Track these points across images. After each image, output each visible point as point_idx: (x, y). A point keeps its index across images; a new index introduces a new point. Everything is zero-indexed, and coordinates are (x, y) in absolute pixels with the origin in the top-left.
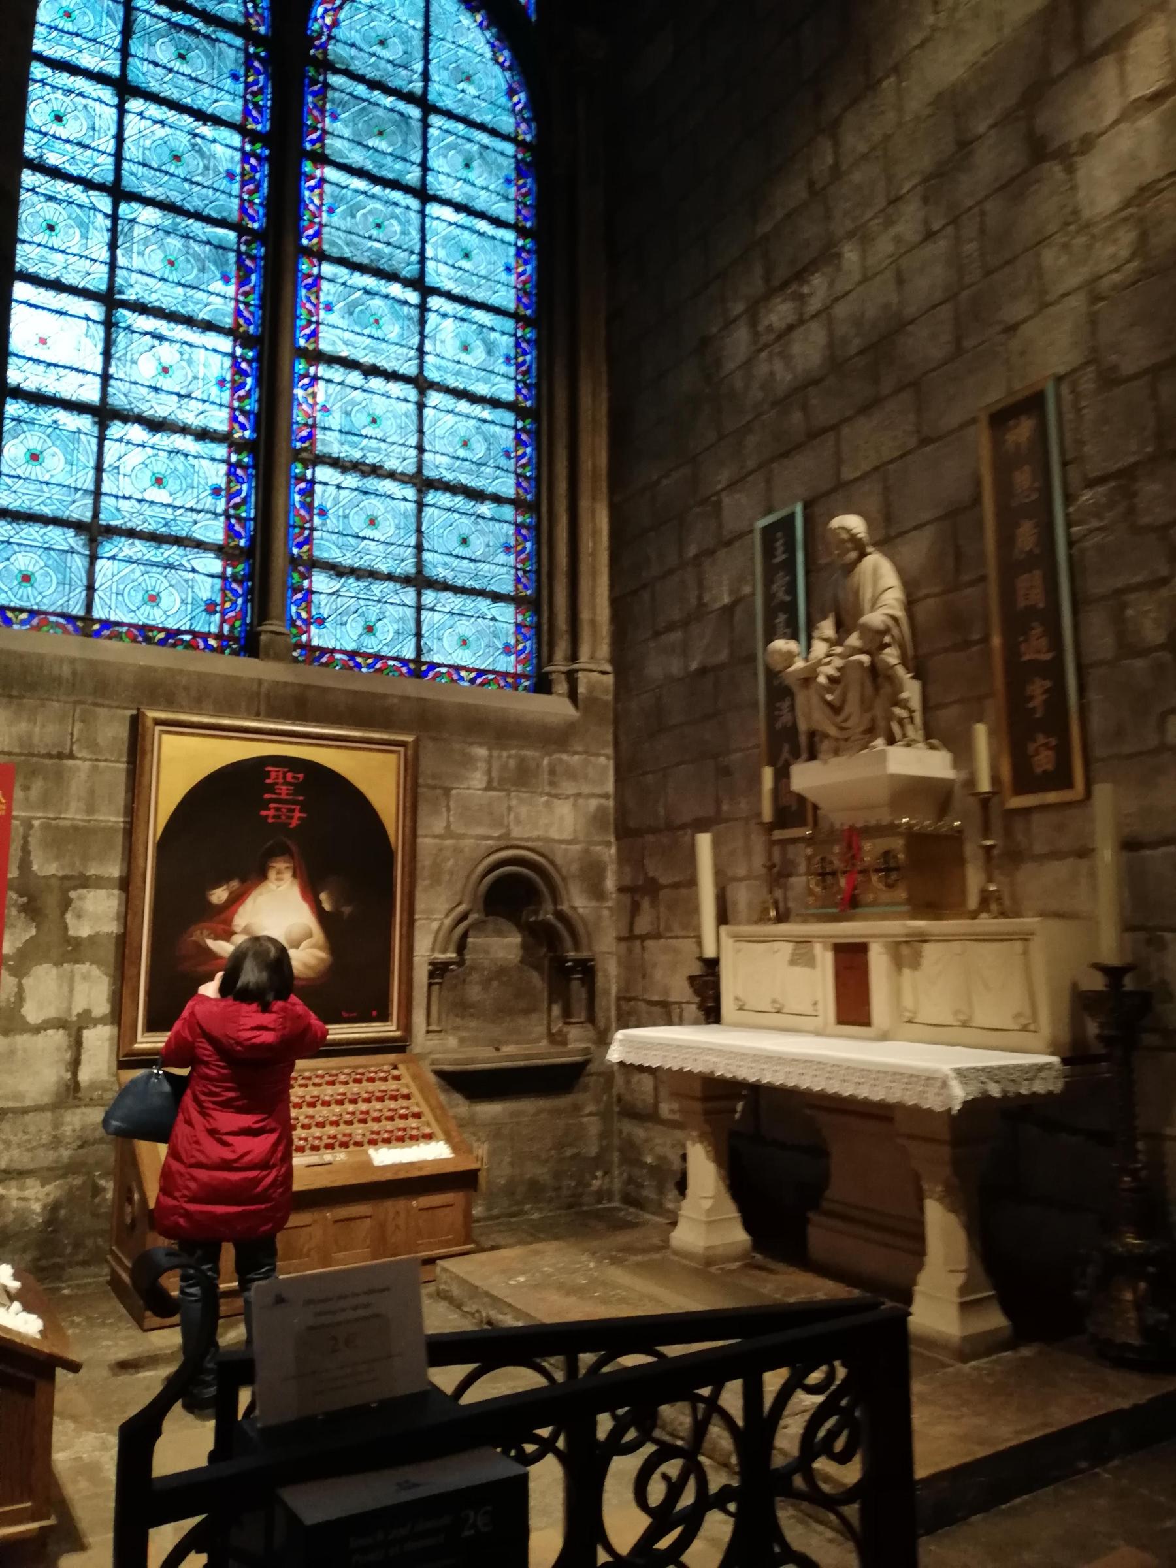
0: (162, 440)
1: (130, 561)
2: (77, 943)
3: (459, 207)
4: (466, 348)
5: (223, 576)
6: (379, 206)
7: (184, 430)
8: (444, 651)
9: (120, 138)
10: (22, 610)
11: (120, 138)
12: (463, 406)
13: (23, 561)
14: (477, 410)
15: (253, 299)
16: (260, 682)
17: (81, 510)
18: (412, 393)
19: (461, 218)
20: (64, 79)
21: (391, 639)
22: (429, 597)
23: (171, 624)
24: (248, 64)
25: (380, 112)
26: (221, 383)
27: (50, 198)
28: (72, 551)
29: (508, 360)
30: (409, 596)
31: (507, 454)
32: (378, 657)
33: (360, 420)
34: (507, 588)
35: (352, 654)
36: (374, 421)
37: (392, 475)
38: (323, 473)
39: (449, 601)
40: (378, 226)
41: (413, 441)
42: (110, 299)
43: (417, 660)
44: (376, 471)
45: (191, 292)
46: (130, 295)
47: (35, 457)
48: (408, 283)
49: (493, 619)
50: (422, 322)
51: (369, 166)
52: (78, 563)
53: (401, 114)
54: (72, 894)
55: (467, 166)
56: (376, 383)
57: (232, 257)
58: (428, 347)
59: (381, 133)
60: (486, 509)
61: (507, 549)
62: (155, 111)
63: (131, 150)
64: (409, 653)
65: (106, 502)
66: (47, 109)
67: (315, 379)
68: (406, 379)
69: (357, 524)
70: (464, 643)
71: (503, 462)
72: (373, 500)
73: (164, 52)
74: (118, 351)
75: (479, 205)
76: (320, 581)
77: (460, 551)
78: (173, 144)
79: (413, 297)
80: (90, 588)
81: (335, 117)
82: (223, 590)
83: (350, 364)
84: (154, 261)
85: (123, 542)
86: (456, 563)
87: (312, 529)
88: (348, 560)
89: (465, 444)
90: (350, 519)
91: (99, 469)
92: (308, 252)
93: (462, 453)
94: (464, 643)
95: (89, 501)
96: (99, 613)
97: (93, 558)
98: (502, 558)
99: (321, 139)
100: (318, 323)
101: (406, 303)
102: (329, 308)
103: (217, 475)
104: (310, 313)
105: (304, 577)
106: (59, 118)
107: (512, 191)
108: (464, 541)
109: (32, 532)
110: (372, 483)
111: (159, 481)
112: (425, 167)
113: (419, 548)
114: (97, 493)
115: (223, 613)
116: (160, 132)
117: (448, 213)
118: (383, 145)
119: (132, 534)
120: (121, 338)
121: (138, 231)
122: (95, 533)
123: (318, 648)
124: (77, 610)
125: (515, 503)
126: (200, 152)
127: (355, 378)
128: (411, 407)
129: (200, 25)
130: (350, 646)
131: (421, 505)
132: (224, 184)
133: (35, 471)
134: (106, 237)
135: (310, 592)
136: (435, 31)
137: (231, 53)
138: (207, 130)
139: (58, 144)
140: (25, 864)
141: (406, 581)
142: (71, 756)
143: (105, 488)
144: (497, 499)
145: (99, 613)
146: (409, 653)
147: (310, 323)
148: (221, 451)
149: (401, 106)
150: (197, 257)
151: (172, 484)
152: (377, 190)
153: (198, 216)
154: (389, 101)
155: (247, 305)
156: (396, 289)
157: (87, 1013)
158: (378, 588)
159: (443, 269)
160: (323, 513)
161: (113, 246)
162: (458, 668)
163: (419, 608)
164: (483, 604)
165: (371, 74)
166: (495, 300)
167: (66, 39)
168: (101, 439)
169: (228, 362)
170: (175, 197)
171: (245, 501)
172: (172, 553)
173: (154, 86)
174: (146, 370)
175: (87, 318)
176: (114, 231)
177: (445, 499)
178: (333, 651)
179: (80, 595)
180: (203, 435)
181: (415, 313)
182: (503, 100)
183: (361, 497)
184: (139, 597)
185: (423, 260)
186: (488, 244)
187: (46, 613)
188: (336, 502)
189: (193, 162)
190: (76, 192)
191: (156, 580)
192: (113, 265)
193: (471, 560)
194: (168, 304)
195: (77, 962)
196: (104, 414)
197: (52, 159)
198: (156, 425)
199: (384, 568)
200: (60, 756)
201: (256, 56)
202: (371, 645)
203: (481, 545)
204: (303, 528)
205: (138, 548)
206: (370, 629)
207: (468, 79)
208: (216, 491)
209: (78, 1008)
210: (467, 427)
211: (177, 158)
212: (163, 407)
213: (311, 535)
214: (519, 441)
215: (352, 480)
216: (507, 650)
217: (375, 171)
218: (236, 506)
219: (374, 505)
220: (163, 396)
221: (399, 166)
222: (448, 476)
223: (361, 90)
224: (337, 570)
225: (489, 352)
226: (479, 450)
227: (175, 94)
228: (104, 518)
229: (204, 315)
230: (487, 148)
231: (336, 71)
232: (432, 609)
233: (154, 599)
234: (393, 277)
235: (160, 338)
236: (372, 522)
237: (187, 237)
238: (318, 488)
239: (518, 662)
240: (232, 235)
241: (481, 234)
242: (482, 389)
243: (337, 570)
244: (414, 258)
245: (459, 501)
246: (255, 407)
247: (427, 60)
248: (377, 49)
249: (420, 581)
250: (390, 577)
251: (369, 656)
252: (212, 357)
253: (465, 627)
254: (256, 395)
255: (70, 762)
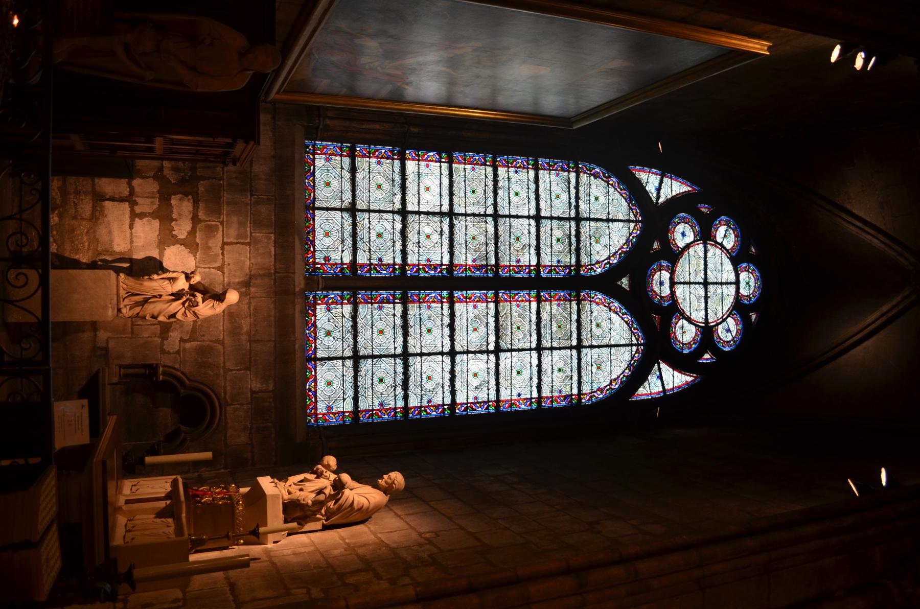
0: (398, 236)
1: (342, 225)
2: (169, 199)
3: (539, 366)
4: (475, 375)
5: (342, 264)
6: (527, 328)
7: (404, 245)
8: (324, 373)
9: (517, 217)
10: (314, 183)
11: (517, 217)
12: (447, 376)
13: (335, 183)
14: (447, 383)
15: (469, 273)
16: (294, 273)
17: (360, 205)
18: (447, 349)
19: (535, 370)
20: (532, 197)
21: (325, 345)
22: (349, 363)
23: (317, 242)
24: (565, 267)
25: (568, 326)
26: (429, 260)
27: (485, 191)
28: (342, 201)
29: (476, 398)
30: (348, 353)
31: (429, 401)
32: (315, 338)
33: (428, 324)
34: (362, 406)
35: (315, 325)
36: (429, 331)
37: (405, 342)
38: (399, 308)
39: (350, 373)
40: (518, 328)
41: (424, 351)
42: (451, 214)
43: (316, 359)
44: (406, 334)
45: (464, 246)
46: (456, 222)
47: (379, 187)
48: (497, 343)
49: (344, 399)
50: (481, 352)
51: (543, 322)
52: (338, 204)
53: (571, 336)
54: (190, 197)
55: (560, 370)
56: (447, 331)
57: (484, 263)
58: (470, 356)
59: (559, 327)
60: (399, 390)
61: (381, 404)
62: (533, 230)
63: (514, 221)
64: (319, 354)
65: (366, 215)
66: (519, 190)
67: (442, 303)
68: (453, 345)
69: (379, 325)
70: (329, 383)
71: (425, 399)
72: (392, 332)
73: (558, 233)
74: (431, 218)
75: (544, 378)
76: (348, 309)
77: (376, 379)
78: (523, 237)
79: (491, 347)
80: (327, 209)
81: (559, 305)
82: (336, 264)
83: (452, 316)
84: (472, 231)
85: (350, 220)
86: (369, 376)
87: (372, 304)
88: (360, 321)
89: (429, 378)
90: (380, 323)
91: (380, 211)
92: (496, 295)
93: (424, 376)
94: (329, 383)
95: (365, 208)
96: (317, 213)
97: (341, 210)
98: (377, 402)
99: (546, 300)
100: (466, 302)
101: (488, 344)
102: (475, 307)
103: (388, 260)
104: (470, 298)
105: (349, 300)
106: (517, 194)
107: (556, 394)
108: (381, 380)
109: (347, 186)
110: (400, 332)
111: (379, 235)
112: (552, 349)
113: (373, 357)
114: (369, 211)
115: (325, 264)
116: (526, 232)
117: (535, 362)
118: (554, 328)
119: (354, 225)
120: (437, 219)
121: (483, 225)
122: (352, 210)
123: (316, 309)
124: (317, 204)
125: (406, 408)
126: (523, 249)
127: (447, 321)
128: (440, 349)
129: (573, 247)
130: (319, 324)
131: (394, 356)
132: (514, 258)
133: (373, 187)
134: (477, 212)
135: (342, 304)
136: (613, 350)
137: (568, 260)
138: (533, 251)
139: (507, 194)
140: (203, 178)
141: (355, 350)
142: (252, 195)
143: (372, 214)
144: (406, 397)
145: (317, 213)
146: (319, 354)
147: (466, 298)
148: (399, 261)
149: (575, 336)
150: (479, 249)
151: (379, 241)
152: (534, 327)
153: (497, 249)
154: (574, 327)
155: (466, 270)
156: (492, 338)
157: (137, 204)
158: (349, 337)
159: (509, 361)
160: (381, 308)
161: (473, 215)
162: (315, 380)
163: (343, 358)
164: (350, 393)
165: (583, 320)
166: (502, 389)
167: (548, 196)
168: (393, 212)
169: (439, 262)
170: (501, 239)
171: (378, 272)
172: (349, 242)
173: (542, 230)
174: (427, 230)
175: (441, 205)
176: (479, 215)
177: (400, 369)
178: (316, 316)
179: (324, 205)
180: (404, 253)
181: (484, 348)
182: (595, 387)
183: (392, 326)
184: (327, 228)
185: (511, 350)
186: (527, 383)
187: (314, 192)
188: (387, 314)
189: (518, 246)
190: (490, 201)
191: (336, 235)
192: (466, 215)
193: (372, 384)
194: (456, 237)
195: (160, 199)
196: (403, 213)
197: (500, 192)
198: (403, 233)
199: (360, 339)
200: (251, 191)
201: (571, 271)
202: (321, 334)
203: (381, 393)
204: (371, 299)
205: (348, 228)
206: (328, 333)
207: (598, 368)
208: (380, 260)
209: (138, 200)
210: (437, 378)
211: (518, 239)
212: (412, 237)
213: (368, 303)
214: (437, 407)
215: (399, 321)
216: (329, 408)
217: (542, 326)
218: (375, 269)
219: (389, 332)
220: (417, 236)
221: (549, 337)
222: (411, 369)
223: (574, 317)
224: (354, 318)
225: (476, 388)
226: (429, 385)
227: (543, 237)
228: (359, 214)
229: (456, 252)
230: (571, 378)
231: (578, 304)
232: (343, 365)
233: (327, 234)
234: (498, 337)
235: (441, 233)
236: (381, 332)
237: (487, 245)
238: (391, 306)
239: (324, 414)
240: (493, 262)
241: (531, 379)
242: (458, 385)
243: (354, 318)
244: (509, 346)
245: (400, 377)
246: (422, 275)
247: (599, 347)
248: (594, 324)
249: (357, 358)
250: (356, 342)
251: (316, 334)
252: (438, 255)
253: (337, 383)
254: (426, 275)
255: (249, 195)
